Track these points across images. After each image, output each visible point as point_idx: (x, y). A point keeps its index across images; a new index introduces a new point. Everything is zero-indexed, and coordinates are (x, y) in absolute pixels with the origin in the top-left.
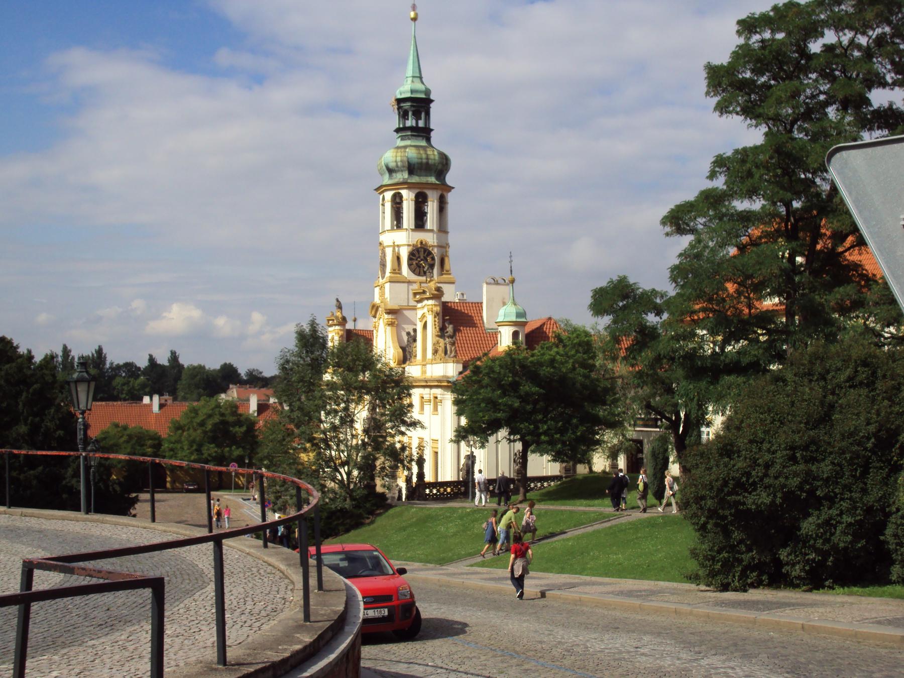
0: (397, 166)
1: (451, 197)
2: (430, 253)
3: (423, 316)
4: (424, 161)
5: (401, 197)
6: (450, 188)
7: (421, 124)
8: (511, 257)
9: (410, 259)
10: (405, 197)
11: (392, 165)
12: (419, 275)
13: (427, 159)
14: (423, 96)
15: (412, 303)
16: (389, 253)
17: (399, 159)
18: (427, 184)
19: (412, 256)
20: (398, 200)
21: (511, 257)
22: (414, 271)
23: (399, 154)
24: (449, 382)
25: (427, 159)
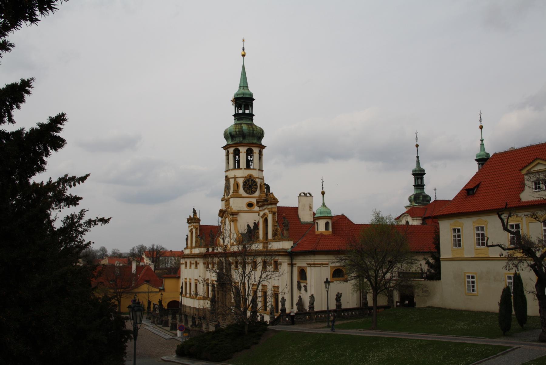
0: (236, 134)
1: (264, 151)
2: (255, 182)
3: (265, 214)
4: (251, 131)
5: (239, 150)
6: (264, 147)
7: (247, 112)
8: (322, 179)
9: (244, 185)
10: (241, 151)
11: (234, 133)
12: (249, 194)
13: (253, 130)
14: (249, 96)
15: (246, 209)
16: (232, 181)
17: (237, 130)
18: (253, 144)
19: (245, 183)
20: (237, 153)
21: (322, 179)
22: (246, 192)
23: (237, 127)
24: (286, 252)
25: (253, 130)
